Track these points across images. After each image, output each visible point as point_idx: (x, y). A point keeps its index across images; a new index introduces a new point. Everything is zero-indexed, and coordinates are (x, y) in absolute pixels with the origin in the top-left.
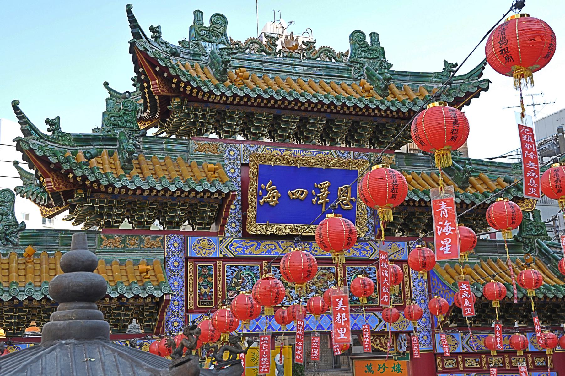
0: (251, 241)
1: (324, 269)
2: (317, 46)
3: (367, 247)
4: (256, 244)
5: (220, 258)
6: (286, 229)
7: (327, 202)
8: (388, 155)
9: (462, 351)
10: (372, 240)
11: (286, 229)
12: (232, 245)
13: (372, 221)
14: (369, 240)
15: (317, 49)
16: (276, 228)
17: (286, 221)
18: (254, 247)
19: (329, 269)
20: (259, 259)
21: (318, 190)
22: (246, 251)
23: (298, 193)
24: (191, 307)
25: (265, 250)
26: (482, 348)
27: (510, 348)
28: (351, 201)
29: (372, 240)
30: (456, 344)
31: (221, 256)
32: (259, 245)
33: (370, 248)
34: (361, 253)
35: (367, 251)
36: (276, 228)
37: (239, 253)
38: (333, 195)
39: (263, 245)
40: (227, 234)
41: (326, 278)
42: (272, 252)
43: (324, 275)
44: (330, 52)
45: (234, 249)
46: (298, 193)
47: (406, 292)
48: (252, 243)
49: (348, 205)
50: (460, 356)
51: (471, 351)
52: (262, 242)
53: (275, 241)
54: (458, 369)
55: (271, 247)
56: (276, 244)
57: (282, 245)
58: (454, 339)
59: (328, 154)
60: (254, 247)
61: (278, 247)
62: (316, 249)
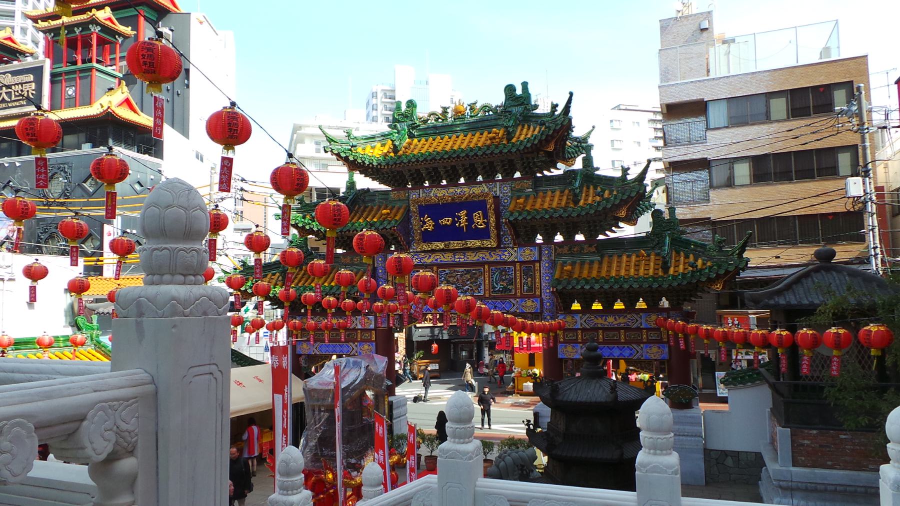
1: (476, 270)
2: (478, 106)
3: (506, 253)
6: (441, 245)
7: (466, 225)
8: (525, 181)
9: (579, 327)
10: (510, 247)
14: (508, 247)
15: (478, 107)
17: (442, 240)
21: (459, 218)
23: (446, 221)
25: (434, 260)
28: (484, 222)
29: (510, 247)
32: (430, 256)
33: (509, 253)
38: (470, 220)
39: (433, 256)
40: (411, 251)
41: (476, 276)
42: (439, 260)
43: (476, 274)
44: (487, 106)
46: (446, 221)
47: (537, 284)
49: (481, 225)
50: (579, 331)
51: (588, 327)
55: (438, 257)
56: (441, 255)
61: (442, 257)
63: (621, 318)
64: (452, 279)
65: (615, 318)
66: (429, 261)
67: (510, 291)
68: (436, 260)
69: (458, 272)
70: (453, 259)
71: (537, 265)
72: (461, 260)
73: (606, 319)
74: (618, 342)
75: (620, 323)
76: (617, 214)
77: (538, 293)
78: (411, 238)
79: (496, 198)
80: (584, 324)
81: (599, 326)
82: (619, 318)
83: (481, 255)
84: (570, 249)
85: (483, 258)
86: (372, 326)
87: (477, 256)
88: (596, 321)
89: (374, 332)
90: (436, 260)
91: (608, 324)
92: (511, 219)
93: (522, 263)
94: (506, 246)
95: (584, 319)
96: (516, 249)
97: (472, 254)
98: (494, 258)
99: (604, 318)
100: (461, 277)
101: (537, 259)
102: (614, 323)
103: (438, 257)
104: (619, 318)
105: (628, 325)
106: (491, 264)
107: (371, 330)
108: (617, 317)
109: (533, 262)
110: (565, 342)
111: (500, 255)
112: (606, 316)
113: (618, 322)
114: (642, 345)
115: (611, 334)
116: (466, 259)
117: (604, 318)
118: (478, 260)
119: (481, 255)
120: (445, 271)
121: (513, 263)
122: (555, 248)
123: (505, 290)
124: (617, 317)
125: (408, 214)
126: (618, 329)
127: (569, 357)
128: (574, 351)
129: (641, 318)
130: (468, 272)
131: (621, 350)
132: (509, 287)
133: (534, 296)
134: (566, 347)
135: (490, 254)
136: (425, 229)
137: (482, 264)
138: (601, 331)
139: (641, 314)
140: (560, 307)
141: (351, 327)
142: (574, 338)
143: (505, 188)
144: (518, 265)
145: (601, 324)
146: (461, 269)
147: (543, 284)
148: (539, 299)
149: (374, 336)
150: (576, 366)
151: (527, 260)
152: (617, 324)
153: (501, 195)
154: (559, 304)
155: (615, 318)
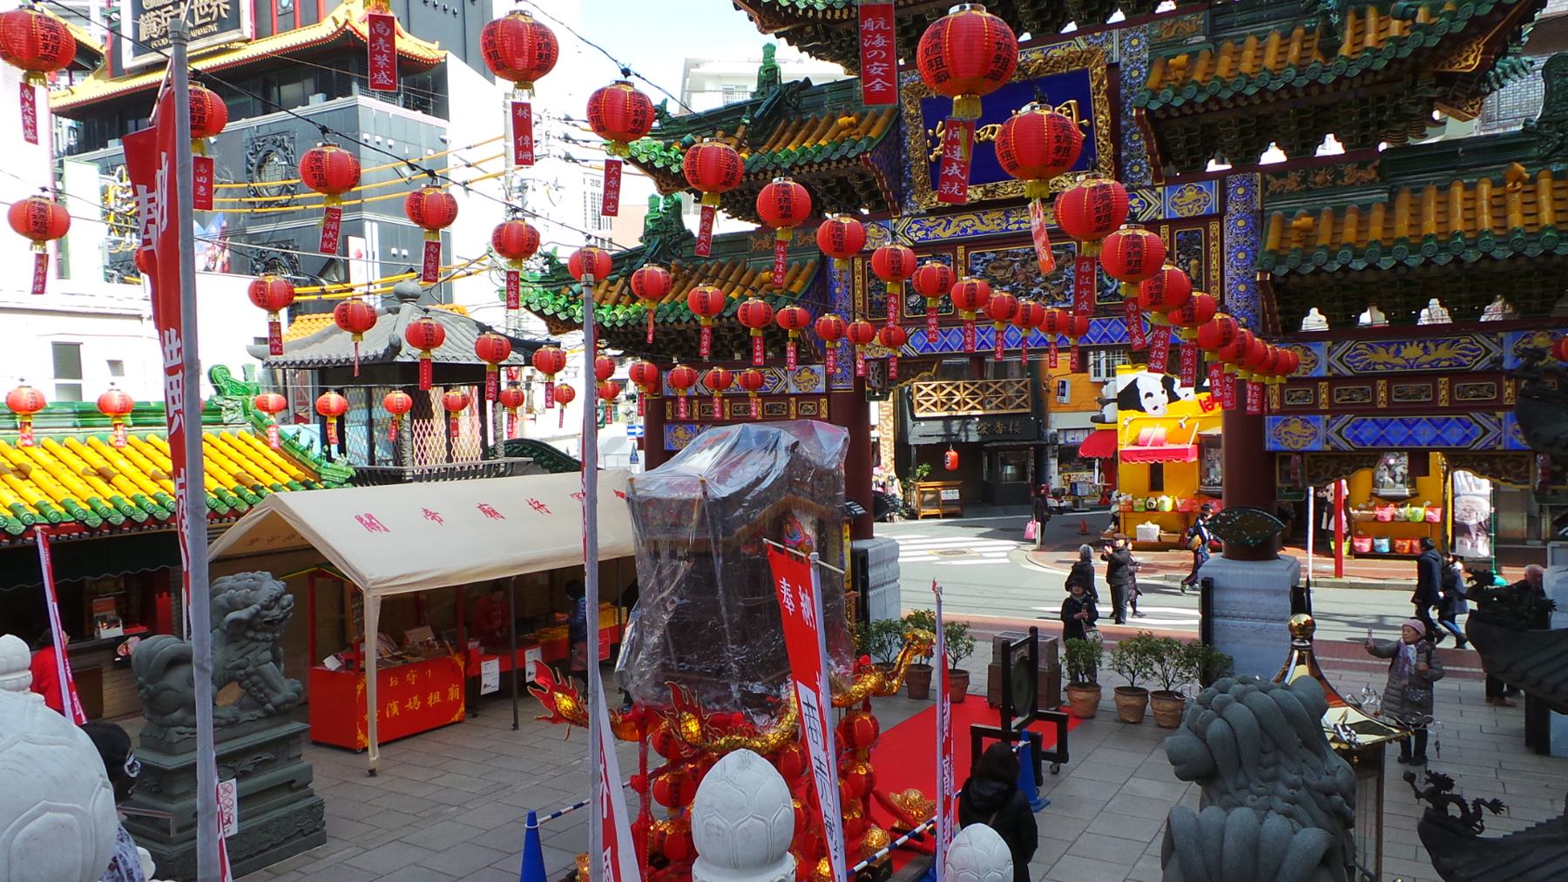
4: (945, 222)
9: (1324, 372)
10: (1146, 187)
12: (910, 228)
14: (1141, 187)
18: (943, 226)
19: (1066, 246)
22: (931, 235)
25: (958, 230)
26: (1377, 367)
27: (1451, 365)
29: (1146, 187)
30: (1312, 362)
32: (949, 222)
33: (1141, 202)
37: (920, 239)
39: (955, 222)
40: (905, 213)
42: (969, 231)
45: (913, 234)
47: (1212, 273)
50: (1323, 384)
51: (1348, 373)
52: (954, 217)
54: (1317, 406)
55: (968, 223)
56: (975, 218)
58: (1309, 353)
59: (1070, 45)
60: (943, 226)
61: (977, 221)
63: (1442, 347)
64: (1001, 272)
69: (1016, 255)
70: (1004, 226)
71: (1214, 227)
73: (1398, 352)
74: (1432, 408)
75: (1439, 360)
76: (1452, 65)
78: (904, 185)
79: (1113, 67)
80: (1338, 365)
81: (1380, 368)
82: (1437, 346)
84: (1304, 180)
86: (821, 388)
88: (1372, 357)
89: (824, 400)
90: (964, 230)
92: (1155, 106)
96: (1159, 190)
99: (1393, 349)
100: (1022, 266)
101: (1216, 210)
102: (1421, 360)
103: (968, 223)
104: (1437, 346)
105: (1461, 364)
107: (818, 396)
108: (1431, 346)
109: (1204, 220)
110: (1285, 411)
112: (1399, 343)
113: (1432, 357)
114: (1500, 414)
115: (1410, 388)
117: (1393, 349)
120: (983, 254)
122: (1263, 178)
124: (1431, 346)
125: (899, 129)
126: (1432, 376)
127: (1295, 447)
128: (1308, 432)
129: (1501, 343)
131: (1438, 427)
134: (1286, 424)
136: (937, 157)
138: (1382, 383)
139: (1501, 334)
140: (1275, 326)
141: (776, 391)
142: (1308, 401)
143: (1135, 42)
145: (1385, 364)
147: (1230, 272)
149: (824, 409)
150: (1310, 470)
151: (1187, 214)
152: (1429, 363)
153: (1124, 59)
154: (1273, 315)
155: (1425, 349)
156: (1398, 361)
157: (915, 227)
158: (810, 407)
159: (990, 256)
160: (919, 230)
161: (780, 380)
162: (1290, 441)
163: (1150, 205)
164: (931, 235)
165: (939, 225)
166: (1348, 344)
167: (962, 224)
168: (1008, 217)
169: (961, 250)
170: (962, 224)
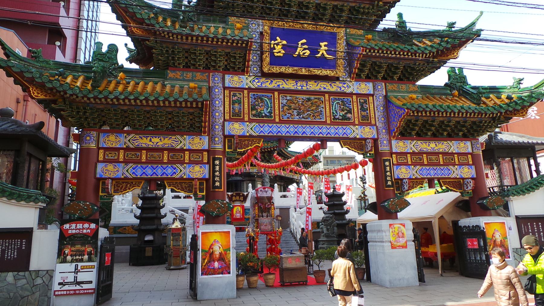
0: (266, 79)
3: (345, 86)
4: (270, 81)
5: (246, 89)
11: (290, 70)
12: (254, 81)
13: (348, 69)
16: (283, 69)
20: (272, 91)
22: (263, 85)
24: (227, 117)
25: (276, 85)
31: (247, 87)
32: (272, 81)
33: (347, 86)
34: (340, 89)
35: (345, 88)
36: (283, 69)
37: (258, 86)
39: (274, 82)
42: (281, 87)
43: (316, 102)
48: (267, 80)
50: (409, 155)
51: (416, 151)
52: (274, 80)
53: (283, 80)
55: (280, 83)
57: (287, 82)
62: (310, 86)
65: (436, 145)
66: (270, 86)
67: (349, 119)
68: (279, 86)
70: (296, 86)
72: (303, 87)
77: (373, 122)
83: (322, 86)
85: (325, 88)
87: (319, 85)
90: (279, 86)
91: (431, 149)
93: (358, 95)
94: (345, 79)
95: (413, 144)
97: (314, 83)
98: (334, 87)
99: (427, 144)
106: (331, 93)
108: (437, 144)
111: (340, 87)
116: (308, 87)
117: (427, 144)
118: (320, 89)
119: (322, 86)
121: (351, 94)
123: (344, 118)
124: (437, 144)
130: (309, 100)
132: (349, 115)
133: (370, 124)
135: (330, 85)
137: (323, 93)
141: (178, 147)
144: (354, 97)
146: (302, 96)
148: (375, 127)
155: (436, 145)
156: (429, 148)
157: (257, 81)
158: (198, 157)
159: (288, 98)
160: (258, 82)
161: (181, 142)
162: (402, 175)
163: (350, 87)
164: (263, 85)
165: (267, 82)
166: (415, 141)
167: (278, 83)
168: (297, 84)
169: (276, 93)
170: (278, 83)
